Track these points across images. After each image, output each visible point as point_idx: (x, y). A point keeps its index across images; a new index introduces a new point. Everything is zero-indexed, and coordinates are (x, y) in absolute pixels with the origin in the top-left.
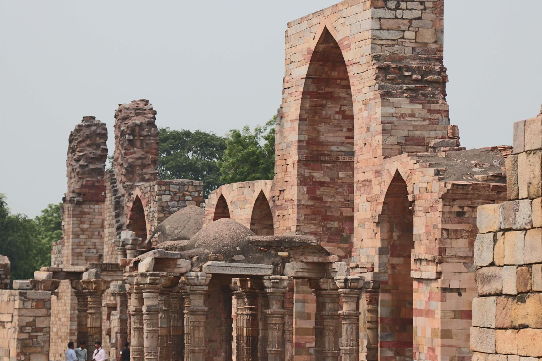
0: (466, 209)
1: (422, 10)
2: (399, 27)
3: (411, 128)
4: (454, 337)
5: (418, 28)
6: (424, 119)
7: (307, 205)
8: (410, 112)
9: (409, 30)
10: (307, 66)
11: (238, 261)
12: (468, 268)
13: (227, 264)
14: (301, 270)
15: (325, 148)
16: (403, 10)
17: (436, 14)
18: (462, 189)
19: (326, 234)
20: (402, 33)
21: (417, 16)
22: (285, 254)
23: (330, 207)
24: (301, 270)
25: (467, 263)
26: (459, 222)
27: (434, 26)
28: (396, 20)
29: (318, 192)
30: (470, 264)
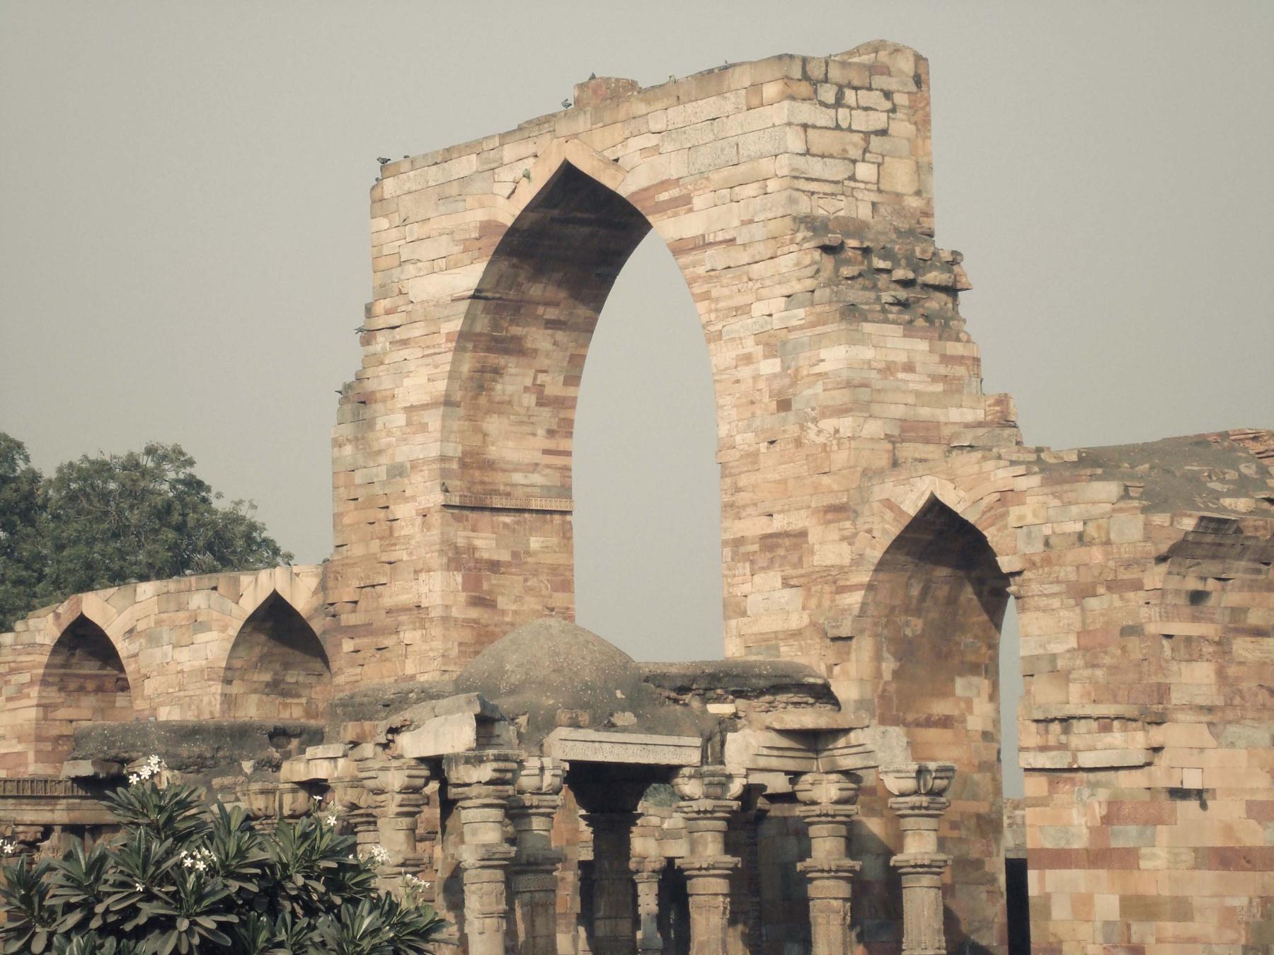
1: (888, 111)
2: (845, 150)
3: (911, 399)
4: (1197, 916)
5: (883, 156)
6: (934, 378)
7: (465, 620)
8: (902, 358)
9: (863, 161)
10: (480, 268)
11: (624, 730)
12: (1216, 736)
13: (603, 736)
14: (765, 752)
16: (851, 108)
17: (916, 123)
18: (1216, 531)
20: (851, 165)
22: (726, 709)
23: (513, 624)
24: (765, 752)
26: (1195, 619)
27: (913, 153)
28: (837, 133)
29: (485, 586)
30: (1220, 727)
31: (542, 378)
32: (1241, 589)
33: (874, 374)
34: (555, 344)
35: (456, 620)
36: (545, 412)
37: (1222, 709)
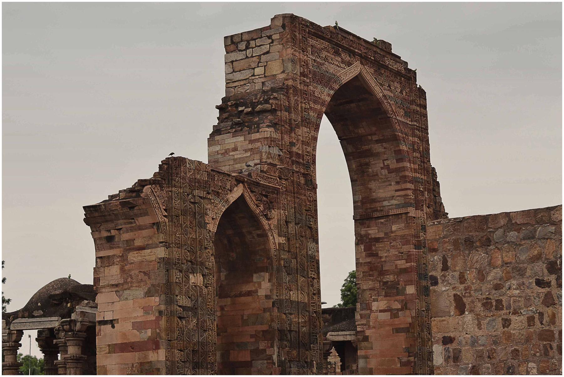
0: (113, 232)
1: (270, 44)
5: (267, 62)
6: (246, 151)
7: (365, 263)
9: (258, 67)
12: (119, 296)
15: (378, 205)
16: (253, 48)
17: (282, 44)
19: (383, 289)
21: (265, 51)
23: (385, 261)
25: (118, 291)
26: (111, 248)
28: (247, 60)
29: (374, 248)
30: (121, 292)
31: (386, 163)
32: (127, 231)
33: (220, 156)
34: (385, 148)
35: (361, 263)
36: (393, 175)
37: (122, 284)
